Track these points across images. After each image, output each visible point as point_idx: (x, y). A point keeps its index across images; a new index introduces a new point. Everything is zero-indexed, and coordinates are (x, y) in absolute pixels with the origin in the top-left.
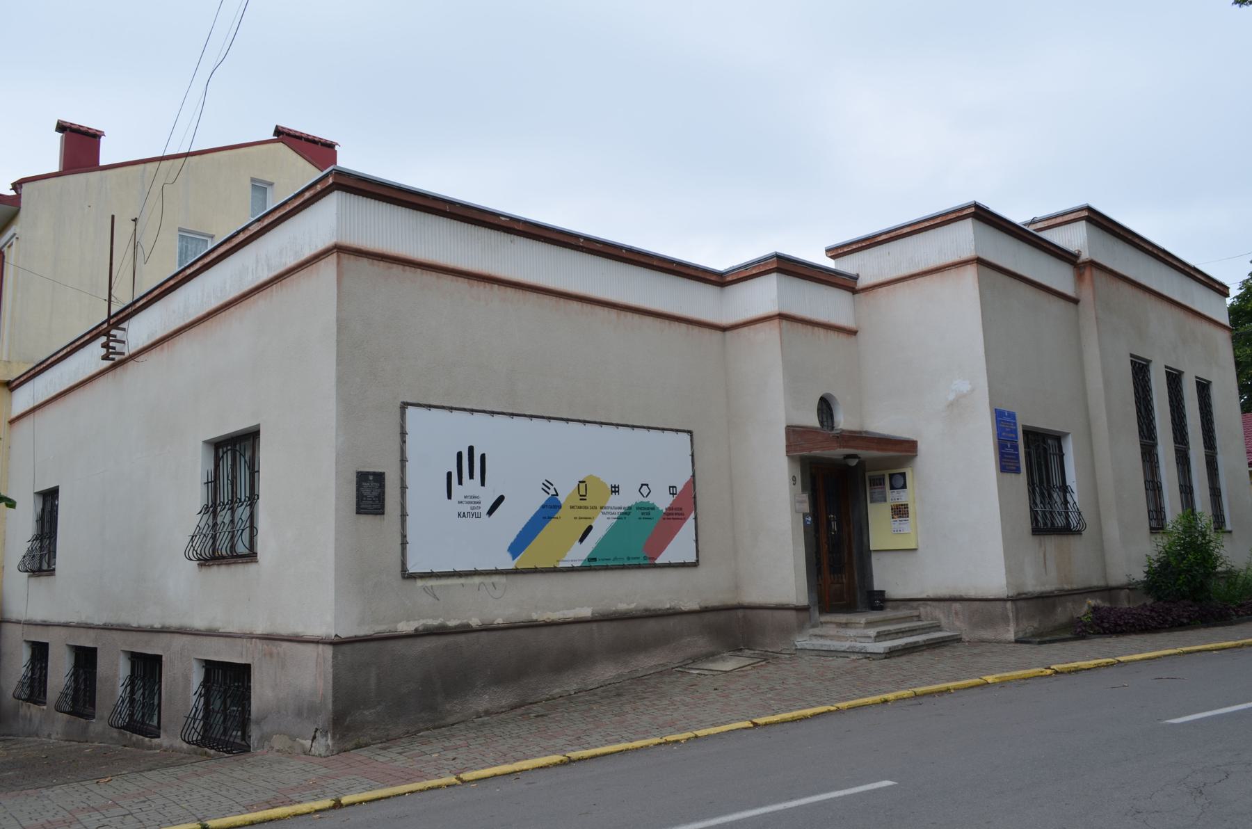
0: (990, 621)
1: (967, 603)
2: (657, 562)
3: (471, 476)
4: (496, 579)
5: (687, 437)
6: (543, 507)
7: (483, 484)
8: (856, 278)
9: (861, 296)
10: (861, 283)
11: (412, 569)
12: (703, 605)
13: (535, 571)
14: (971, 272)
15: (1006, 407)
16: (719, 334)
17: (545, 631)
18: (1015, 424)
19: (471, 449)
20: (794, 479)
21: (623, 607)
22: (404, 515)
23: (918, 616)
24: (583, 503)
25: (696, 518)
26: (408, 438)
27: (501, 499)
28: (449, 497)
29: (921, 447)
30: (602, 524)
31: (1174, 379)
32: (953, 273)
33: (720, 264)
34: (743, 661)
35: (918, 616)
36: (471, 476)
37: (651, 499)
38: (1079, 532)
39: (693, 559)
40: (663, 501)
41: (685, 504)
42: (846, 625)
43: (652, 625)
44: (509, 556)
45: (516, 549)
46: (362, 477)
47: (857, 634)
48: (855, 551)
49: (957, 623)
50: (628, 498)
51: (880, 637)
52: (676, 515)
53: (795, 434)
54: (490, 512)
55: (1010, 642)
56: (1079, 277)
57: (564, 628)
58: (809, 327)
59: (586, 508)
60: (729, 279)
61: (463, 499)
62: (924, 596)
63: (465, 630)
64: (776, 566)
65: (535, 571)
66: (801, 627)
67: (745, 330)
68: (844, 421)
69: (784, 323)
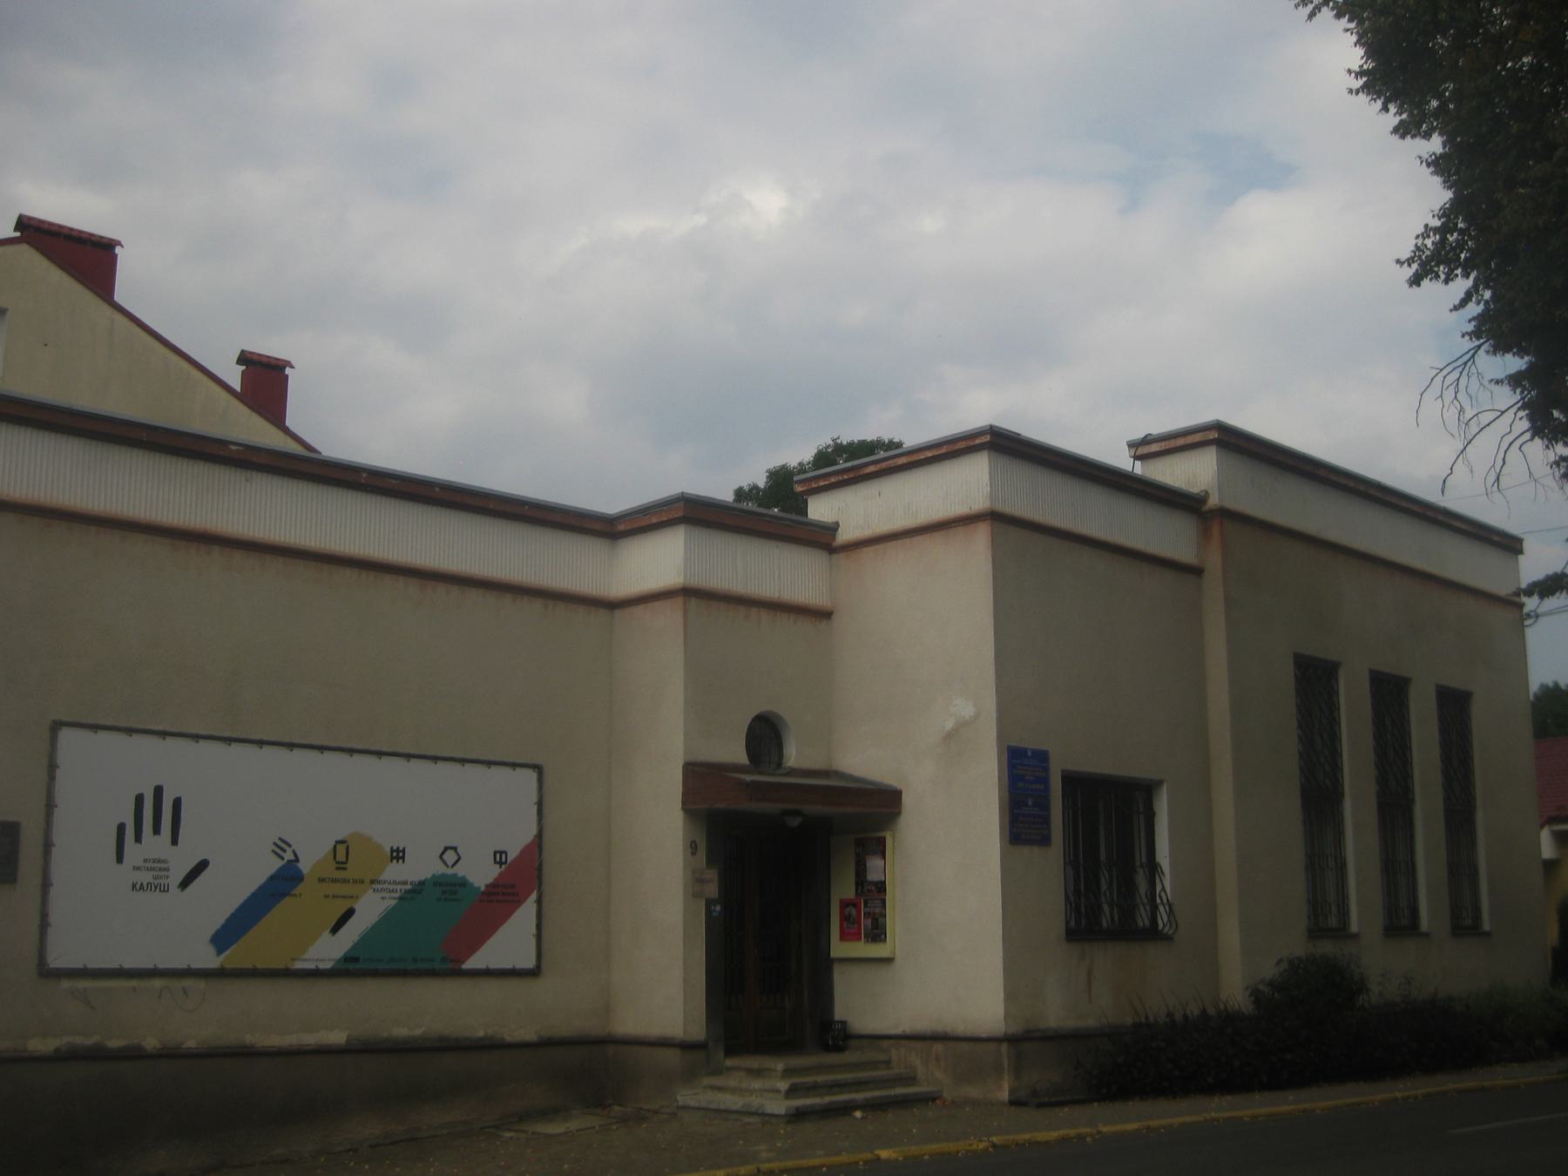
2: (465, 966)
3: (157, 830)
4: (188, 983)
5: (532, 776)
6: (272, 878)
7: (175, 841)
8: (833, 528)
9: (840, 558)
10: (843, 536)
11: (56, 960)
15: (1030, 742)
18: (1046, 769)
19: (158, 791)
20: (693, 847)
21: (401, 1032)
22: (46, 885)
25: (539, 902)
27: (202, 866)
29: (907, 800)
30: (371, 909)
31: (1389, 692)
32: (960, 532)
33: (610, 502)
36: (157, 830)
37: (460, 870)
38: (1168, 938)
39: (530, 963)
40: (481, 873)
41: (521, 877)
42: (758, 1073)
44: (211, 950)
45: (224, 938)
47: (762, 1089)
50: (421, 867)
51: (793, 1092)
52: (502, 897)
53: (699, 776)
54: (185, 884)
56: (1205, 533)
58: (742, 609)
59: (345, 881)
60: (622, 527)
61: (140, 863)
62: (898, 1031)
63: (134, 1054)
67: (639, 610)
68: (795, 754)
69: (693, 602)
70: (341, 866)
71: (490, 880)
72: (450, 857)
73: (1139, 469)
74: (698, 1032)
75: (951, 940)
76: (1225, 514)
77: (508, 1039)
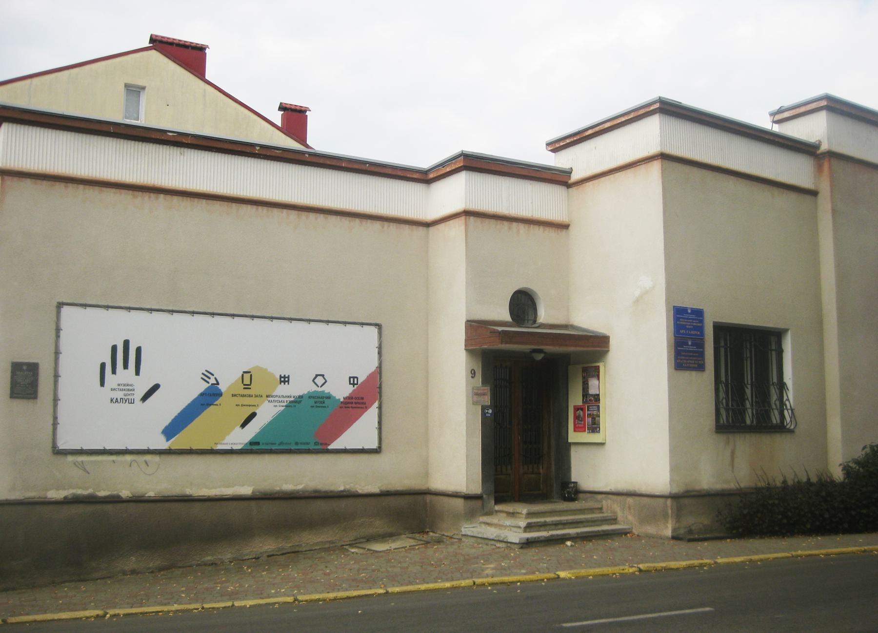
0: (649, 517)
1: (638, 498)
2: (330, 447)
3: (126, 366)
4: (148, 458)
5: (374, 331)
6: (202, 394)
7: (137, 373)
8: (569, 172)
9: (573, 190)
10: (575, 177)
11: (62, 445)
12: (384, 488)
13: (190, 452)
14: (656, 168)
15: (690, 303)
16: (421, 230)
17: (197, 505)
18: (702, 321)
19: (126, 343)
20: (473, 373)
21: (288, 487)
22: (56, 400)
23: (601, 509)
24: (247, 392)
25: (380, 408)
26: (62, 333)
27: (156, 387)
28: (102, 384)
29: (612, 342)
30: (267, 413)
33: (425, 163)
34: (412, 542)
35: (601, 509)
36: (126, 366)
37: (326, 389)
38: (791, 431)
39: (375, 445)
40: (340, 390)
41: (366, 394)
42: (512, 515)
43: (319, 505)
44: (163, 438)
45: (170, 431)
46: (16, 367)
47: (510, 525)
48: (553, 442)
49: (630, 518)
50: (300, 386)
51: (529, 527)
52: (355, 405)
53: (476, 328)
54: (145, 398)
55: (667, 538)
56: (819, 168)
57: (218, 503)
58: (506, 223)
59: (250, 396)
60: (431, 176)
61: (116, 387)
62: (607, 489)
63: (115, 500)
64: (453, 457)
65: (190, 452)
66: (471, 515)
67: (442, 227)
68: (545, 315)
69: (472, 218)
70: (247, 387)
71: (347, 394)
72: (320, 381)
73: (776, 128)
74: (476, 488)
76: (832, 155)
77: (360, 492)
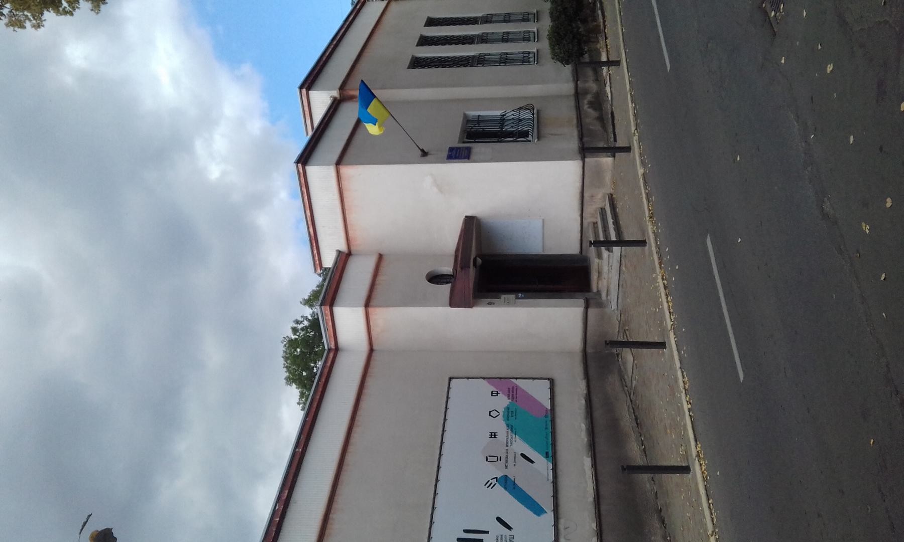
2: (549, 408)
4: (561, 527)
5: (453, 381)
6: (506, 488)
7: (487, 532)
10: (343, 247)
16: (374, 354)
20: (490, 304)
24: (503, 459)
25: (517, 378)
27: (499, 519)
30: (520, 446)
31: (424, 41)
32: (344, 183)
37: (501, 410)
40: (502, 402)
41: (503, 383)
42: (600, 273)
43: (597, 414)
44: (543, 516)
45: (538, 510)
50: (500, 426)
52: (513, 393)
53: (455, 302)
54: (509, 528)
57: (600, 478)
62: (579, 219)
66: (601, 305)
68: (448, 269)
70: (499, 459)
71: (506, 398)
72: (494, 414)
74: (581, 302)
75: (535, 194)
76: (342, 88)
77: (585, 392)
